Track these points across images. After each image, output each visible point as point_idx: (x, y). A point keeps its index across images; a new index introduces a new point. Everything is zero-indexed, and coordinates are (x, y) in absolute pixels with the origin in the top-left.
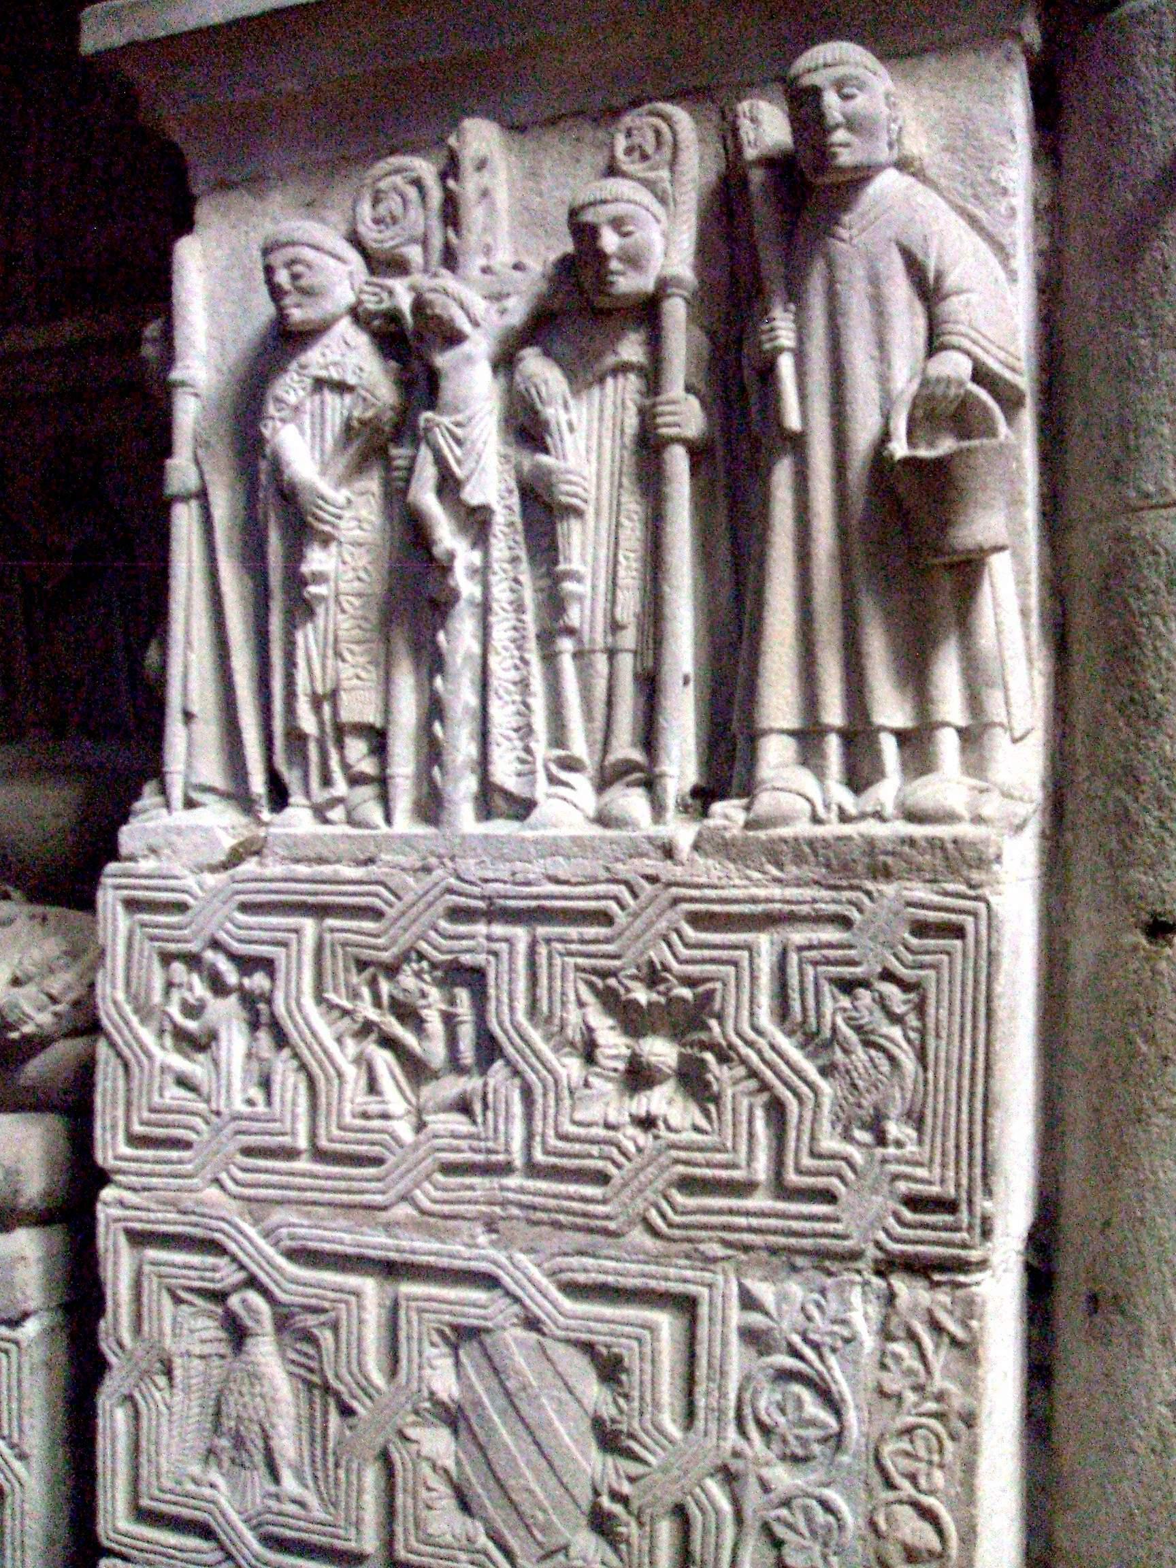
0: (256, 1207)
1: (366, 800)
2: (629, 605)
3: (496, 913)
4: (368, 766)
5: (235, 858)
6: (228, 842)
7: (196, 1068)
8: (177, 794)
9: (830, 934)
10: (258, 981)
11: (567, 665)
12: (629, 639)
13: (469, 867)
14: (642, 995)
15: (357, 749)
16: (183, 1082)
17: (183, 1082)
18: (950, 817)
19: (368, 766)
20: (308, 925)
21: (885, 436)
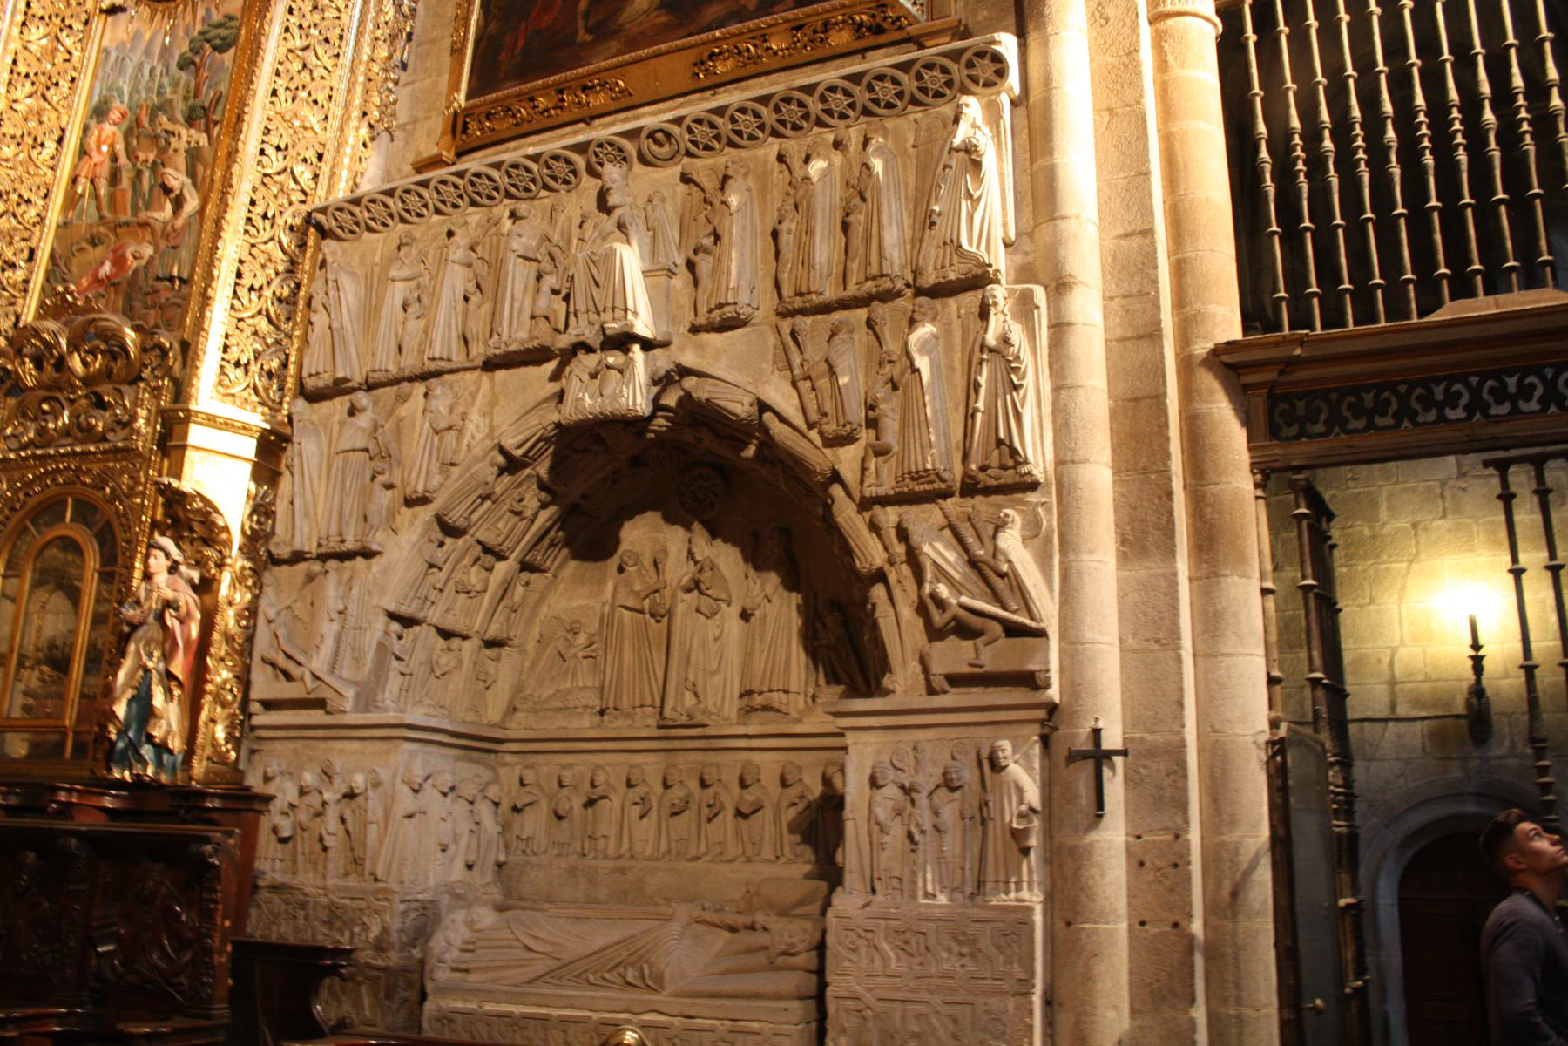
0: (870, 990)
1: (897, 894)
2: (958, 851)
3: (928, 920)
4: (898, 886)
5: (865, 906)
6: (862, 903)
7: (853, 957)
8: (848, 890)
9: (1001, 925)
10: (870, 935)
11: (943, 866)
12: (957, 860)
13: (922, 910)
14: (961, 938)
15: (895, 882)
16: (850, 960)
17: (850, 960)
18: (1024, 901)
19: (898, 886)
20: (882, 923)
21: (1011, 822)
